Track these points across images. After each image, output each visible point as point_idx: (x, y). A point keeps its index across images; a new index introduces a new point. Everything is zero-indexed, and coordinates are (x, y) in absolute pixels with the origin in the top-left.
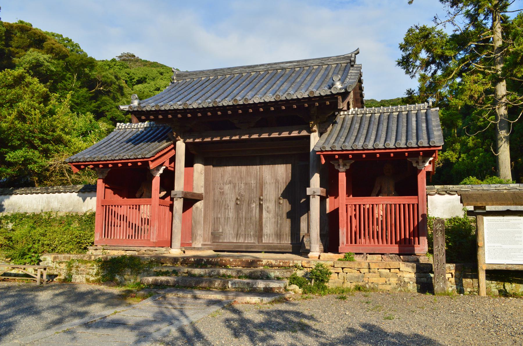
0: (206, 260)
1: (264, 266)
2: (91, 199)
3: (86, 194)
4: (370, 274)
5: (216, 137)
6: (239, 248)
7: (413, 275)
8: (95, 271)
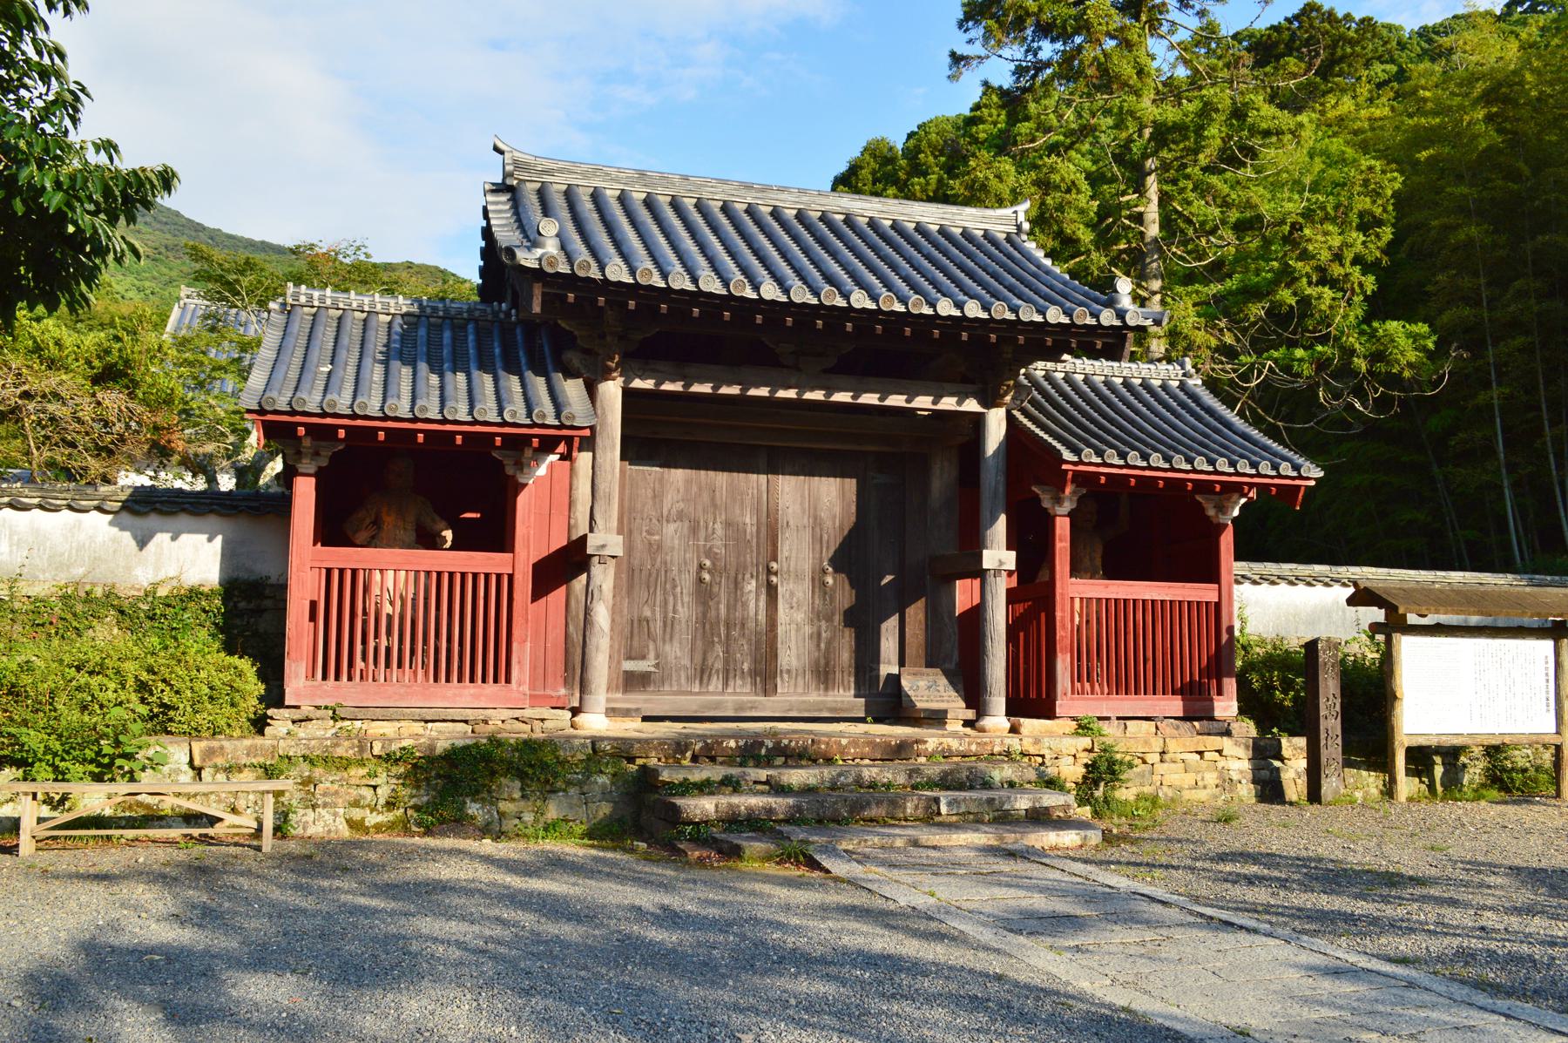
0: (770, 745)
1: (930, 757)
2: (174, 539)
3: (153, 520)
4: (1165, 765)
5: (730, 384)
6: (710, 709)
7: (1246, 765)
8: (384, 793)
